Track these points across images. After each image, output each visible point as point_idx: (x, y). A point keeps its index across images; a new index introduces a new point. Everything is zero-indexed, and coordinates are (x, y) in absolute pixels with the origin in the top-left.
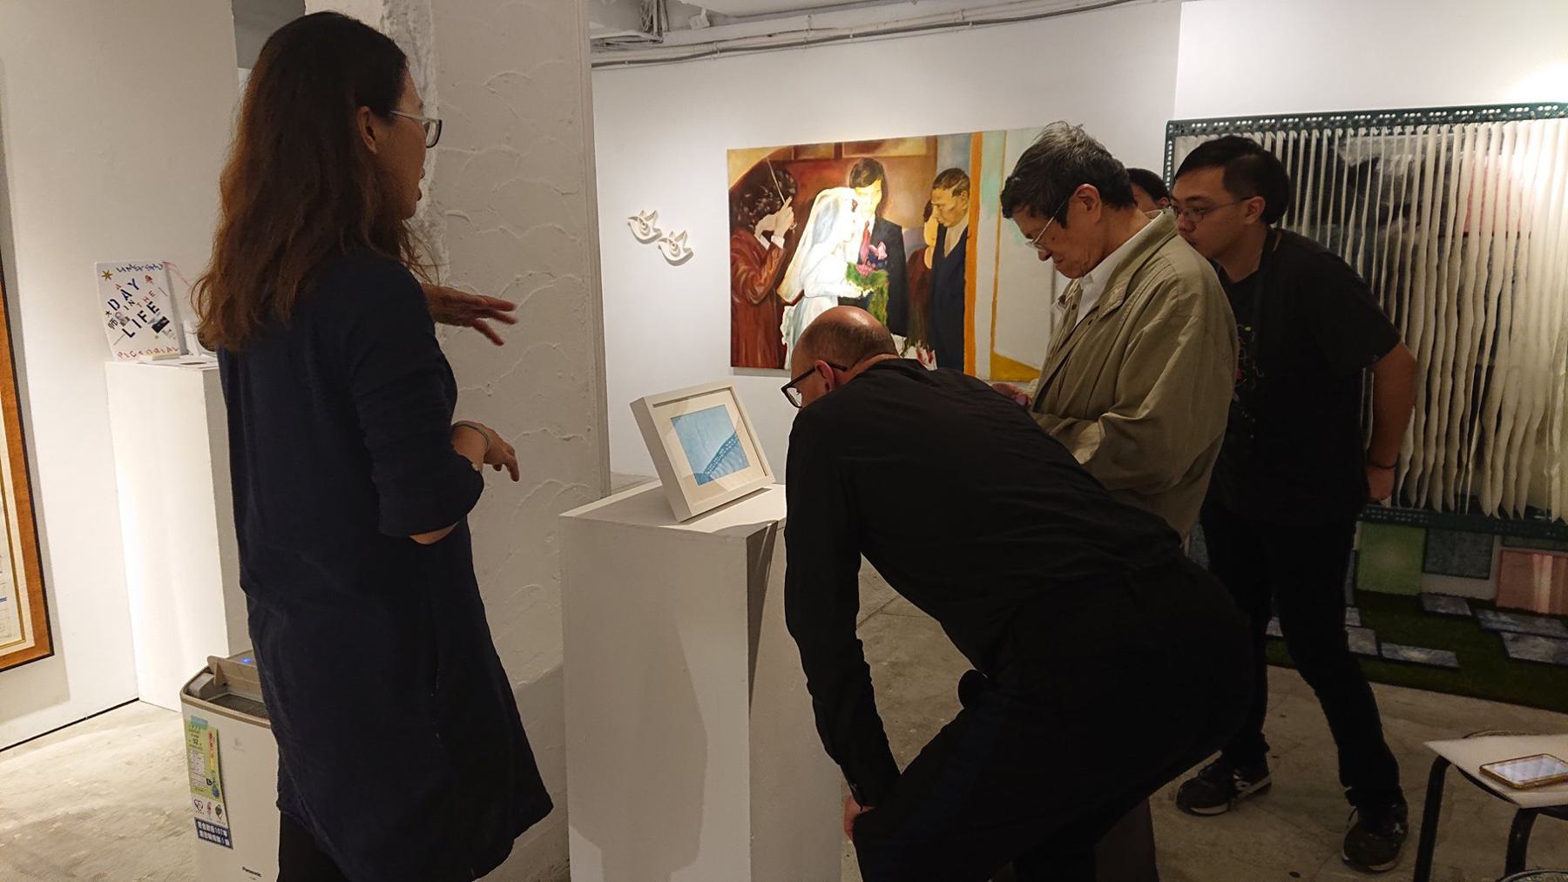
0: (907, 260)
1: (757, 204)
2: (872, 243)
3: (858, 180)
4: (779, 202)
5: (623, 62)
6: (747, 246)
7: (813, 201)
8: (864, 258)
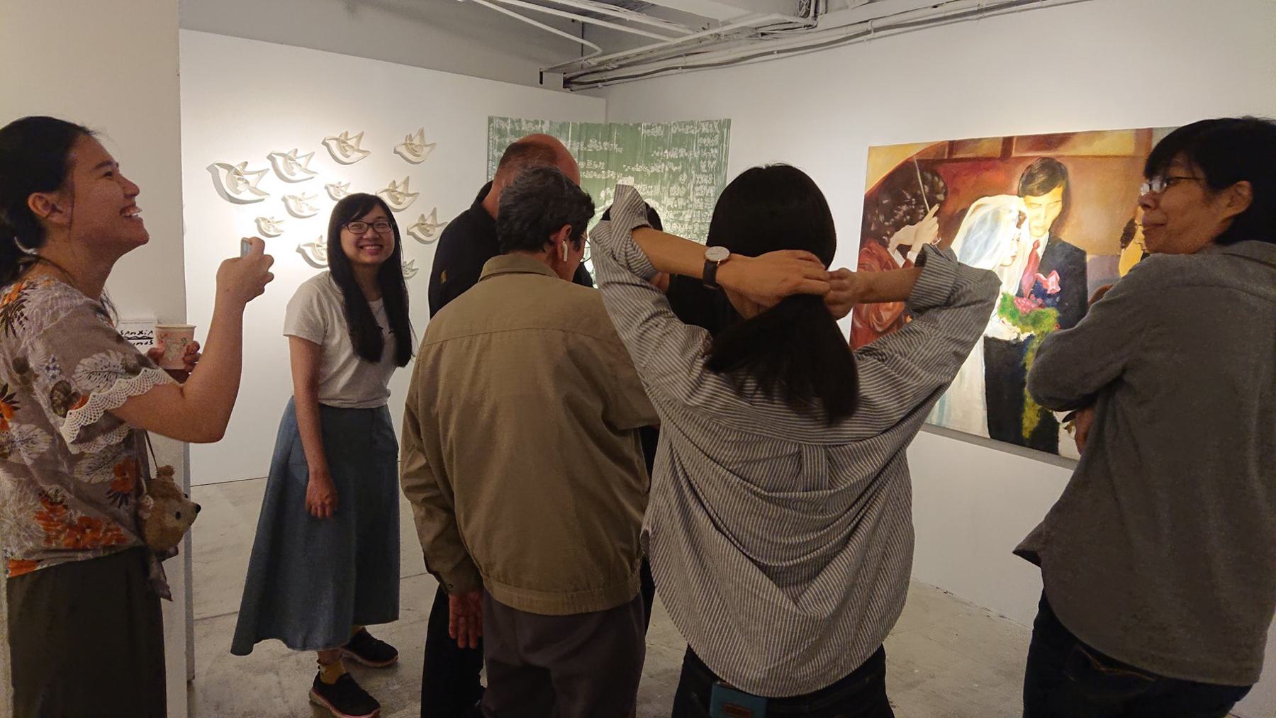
0: (1090, 298)
1: (896, 211)
2: (1040, 270)
3: (1030, 186)
4: (922, 211)
5: (772, 53)
6: (877, 263)
7: (964, 212)
8: (1027, 289)
